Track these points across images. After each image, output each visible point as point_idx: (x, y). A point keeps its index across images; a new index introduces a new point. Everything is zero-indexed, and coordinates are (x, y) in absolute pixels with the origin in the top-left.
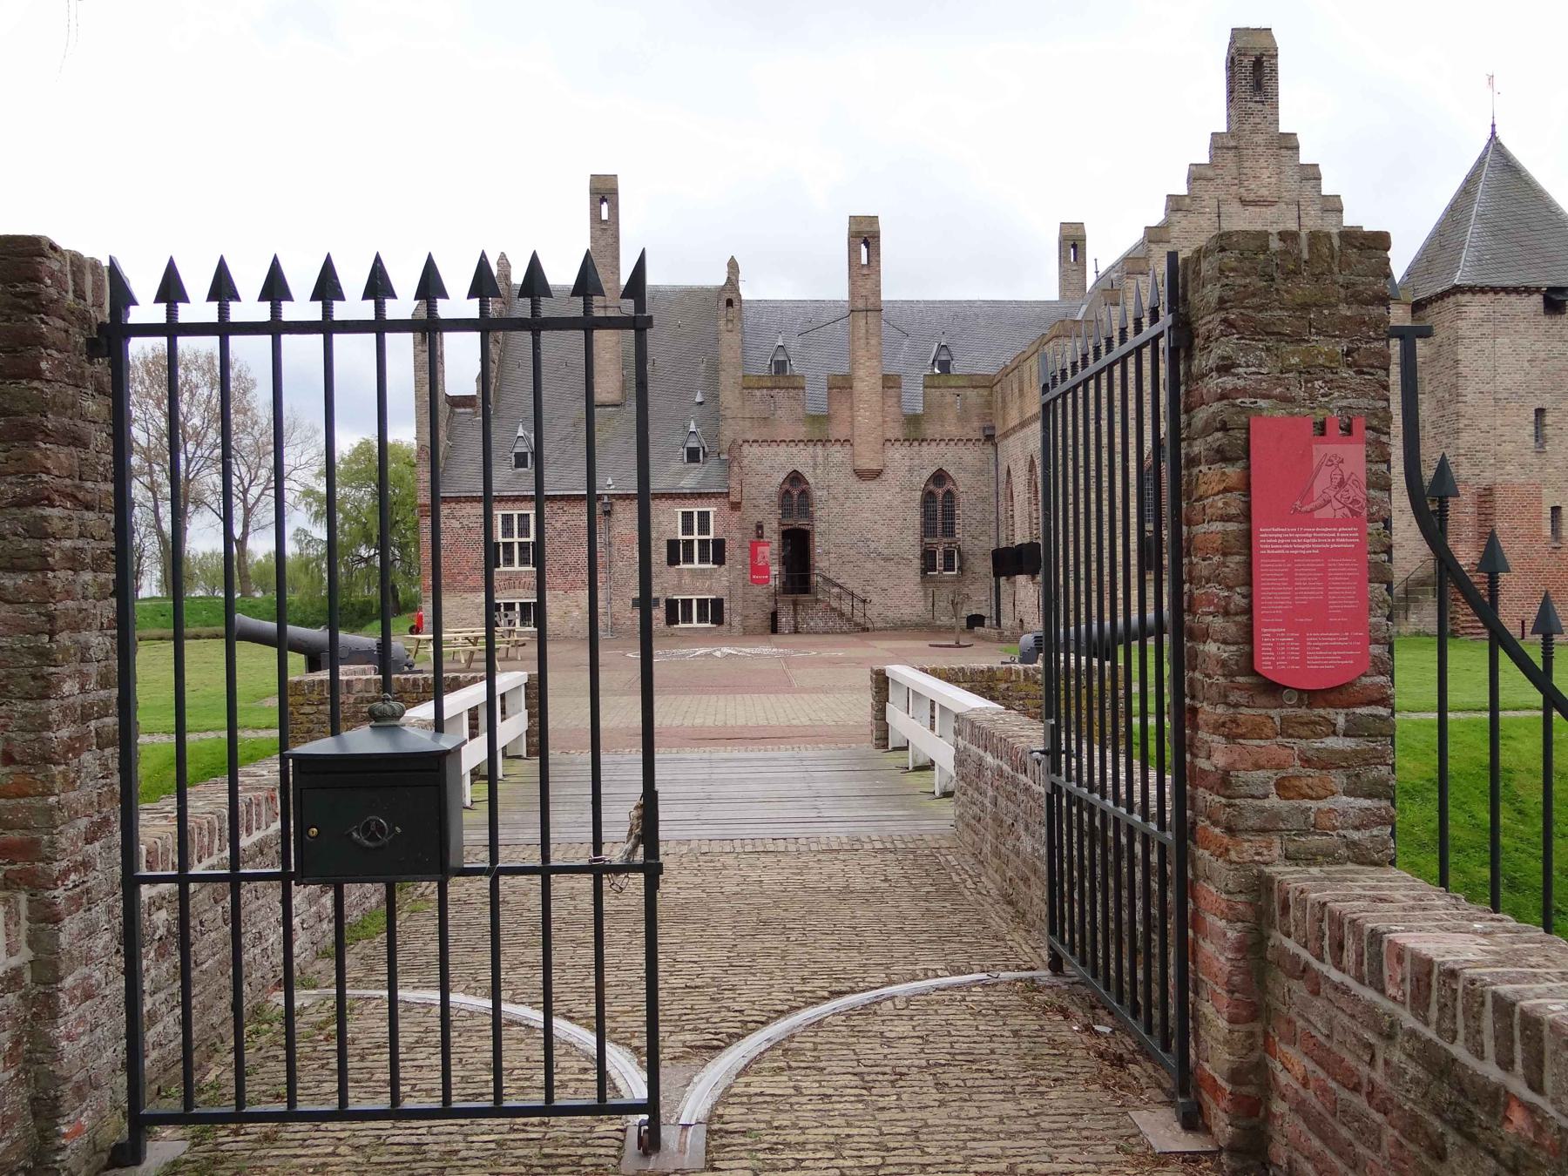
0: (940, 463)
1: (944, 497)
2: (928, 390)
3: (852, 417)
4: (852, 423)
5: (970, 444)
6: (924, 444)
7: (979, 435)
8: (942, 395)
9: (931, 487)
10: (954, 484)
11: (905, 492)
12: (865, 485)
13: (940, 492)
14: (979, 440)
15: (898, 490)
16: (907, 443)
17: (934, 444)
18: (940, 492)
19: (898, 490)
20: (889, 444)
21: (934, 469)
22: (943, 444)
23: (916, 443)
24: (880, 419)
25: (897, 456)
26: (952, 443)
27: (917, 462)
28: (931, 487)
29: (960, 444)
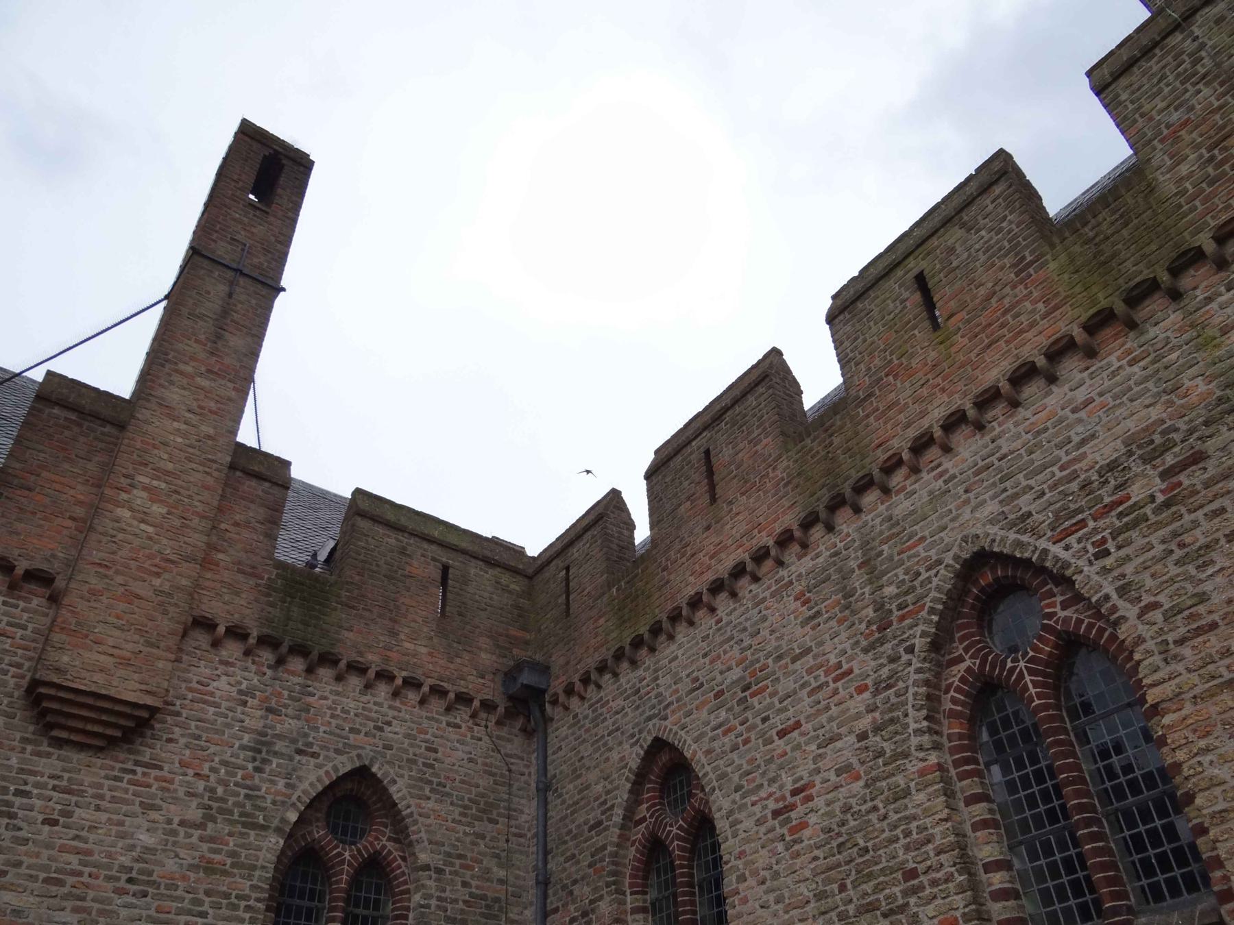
0: (366, 748)
1: (355, 882)
2: (363, 524)
3: (95, 510)
4: (86, 527)
5: (462, 715)
6: (325, 673)
7: (489, 689)
8: (403, 551)
9: (319, 833)
10: (401, 834)
11: (219, 827)
12: (51, 764)
13: (347, 856)
14: (488, 706)
15: (194, 814)
16: (267, 656)
17: (355, 681)
18: (347, 856)
19: (194, 814)
20: (201, 639)
21: (345, 765)
22: (383, 690)
23: (297, 664)
24: (197, 540)
25: (222, 685)
26: (413, 696)
27: (290, 725)
28: (319, 833)
29: (437, 705)
